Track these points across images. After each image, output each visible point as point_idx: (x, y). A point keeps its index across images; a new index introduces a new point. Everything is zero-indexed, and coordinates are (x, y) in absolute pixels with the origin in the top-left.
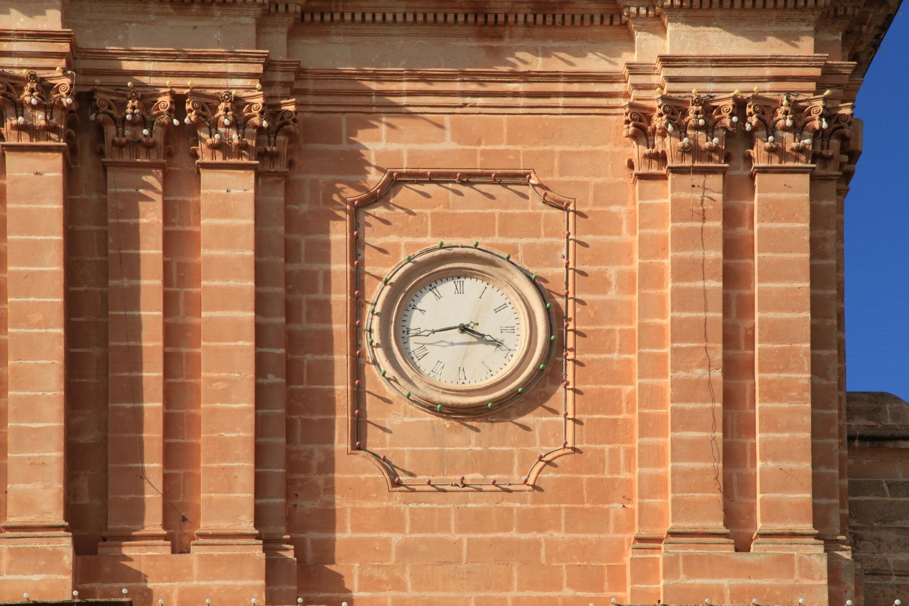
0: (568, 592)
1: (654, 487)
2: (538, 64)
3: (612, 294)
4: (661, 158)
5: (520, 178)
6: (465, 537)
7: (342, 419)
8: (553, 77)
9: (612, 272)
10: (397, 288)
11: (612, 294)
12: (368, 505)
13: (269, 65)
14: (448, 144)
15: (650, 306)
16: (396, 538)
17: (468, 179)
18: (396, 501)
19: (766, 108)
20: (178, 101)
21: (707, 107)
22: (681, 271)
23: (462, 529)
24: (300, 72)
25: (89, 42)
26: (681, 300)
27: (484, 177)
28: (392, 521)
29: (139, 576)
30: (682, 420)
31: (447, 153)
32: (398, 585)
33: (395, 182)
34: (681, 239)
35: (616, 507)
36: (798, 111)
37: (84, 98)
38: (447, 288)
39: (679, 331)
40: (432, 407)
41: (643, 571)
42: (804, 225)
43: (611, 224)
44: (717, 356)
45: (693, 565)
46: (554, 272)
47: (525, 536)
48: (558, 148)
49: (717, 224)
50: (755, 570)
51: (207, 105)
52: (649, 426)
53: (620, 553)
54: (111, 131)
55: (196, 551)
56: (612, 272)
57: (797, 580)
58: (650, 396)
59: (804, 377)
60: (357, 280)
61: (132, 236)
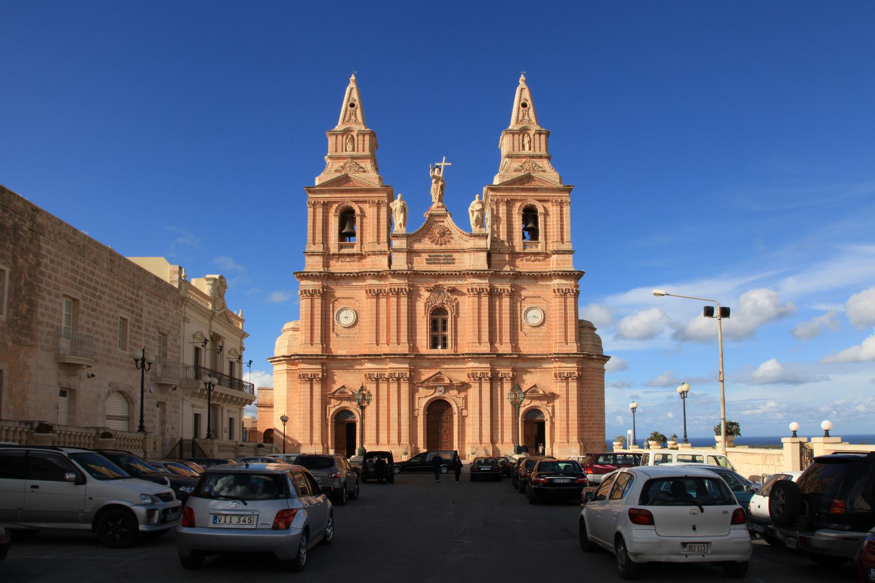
1: (556, 336)
2: (542, 283)
3: (551, 312)
4: (557, 295)
5: (540, 297)
7: (519, 328)
8: (544, 285)
9: (551, 309)
10: (526, 311)
11: (551, 312)
13: (511, 285)
14: (531, 293)
15: (556, 314)
17: (534, 297)
18: (526, 338)
19: (569, 290)
20: (501, 289)
21: (562, 290)
22: (560, 309)
24: (514, 285)
25: (491, 283)
26: (559, 313)
27: (536, 297)
28: (525, 340)
29: (496, 348)
30: (560, 328)
31: (531, 294)
33: (525, 298)
34: (559, 306)
35: (552, 338)
36: (572, 290)
37: (491, 289)
38: (531, 311)
39: (560, 317)
40: (530, 326)
41: (555, 347)
42: (573, 304)
43: (551, 303)
44: (564, 320)
45: (561, 346)
46: (544, 309)
48: (544, 293)
49: (563, 304)
50: (568, 347)
51: (504, 290)
52: (556, 329)
53: (552, 344)
54: (493, 293)
56: (551, 309)
57: (574, 348)
58: (556, 325)
59: (574, 323)
60: (521, 310)
61: (495, 306)
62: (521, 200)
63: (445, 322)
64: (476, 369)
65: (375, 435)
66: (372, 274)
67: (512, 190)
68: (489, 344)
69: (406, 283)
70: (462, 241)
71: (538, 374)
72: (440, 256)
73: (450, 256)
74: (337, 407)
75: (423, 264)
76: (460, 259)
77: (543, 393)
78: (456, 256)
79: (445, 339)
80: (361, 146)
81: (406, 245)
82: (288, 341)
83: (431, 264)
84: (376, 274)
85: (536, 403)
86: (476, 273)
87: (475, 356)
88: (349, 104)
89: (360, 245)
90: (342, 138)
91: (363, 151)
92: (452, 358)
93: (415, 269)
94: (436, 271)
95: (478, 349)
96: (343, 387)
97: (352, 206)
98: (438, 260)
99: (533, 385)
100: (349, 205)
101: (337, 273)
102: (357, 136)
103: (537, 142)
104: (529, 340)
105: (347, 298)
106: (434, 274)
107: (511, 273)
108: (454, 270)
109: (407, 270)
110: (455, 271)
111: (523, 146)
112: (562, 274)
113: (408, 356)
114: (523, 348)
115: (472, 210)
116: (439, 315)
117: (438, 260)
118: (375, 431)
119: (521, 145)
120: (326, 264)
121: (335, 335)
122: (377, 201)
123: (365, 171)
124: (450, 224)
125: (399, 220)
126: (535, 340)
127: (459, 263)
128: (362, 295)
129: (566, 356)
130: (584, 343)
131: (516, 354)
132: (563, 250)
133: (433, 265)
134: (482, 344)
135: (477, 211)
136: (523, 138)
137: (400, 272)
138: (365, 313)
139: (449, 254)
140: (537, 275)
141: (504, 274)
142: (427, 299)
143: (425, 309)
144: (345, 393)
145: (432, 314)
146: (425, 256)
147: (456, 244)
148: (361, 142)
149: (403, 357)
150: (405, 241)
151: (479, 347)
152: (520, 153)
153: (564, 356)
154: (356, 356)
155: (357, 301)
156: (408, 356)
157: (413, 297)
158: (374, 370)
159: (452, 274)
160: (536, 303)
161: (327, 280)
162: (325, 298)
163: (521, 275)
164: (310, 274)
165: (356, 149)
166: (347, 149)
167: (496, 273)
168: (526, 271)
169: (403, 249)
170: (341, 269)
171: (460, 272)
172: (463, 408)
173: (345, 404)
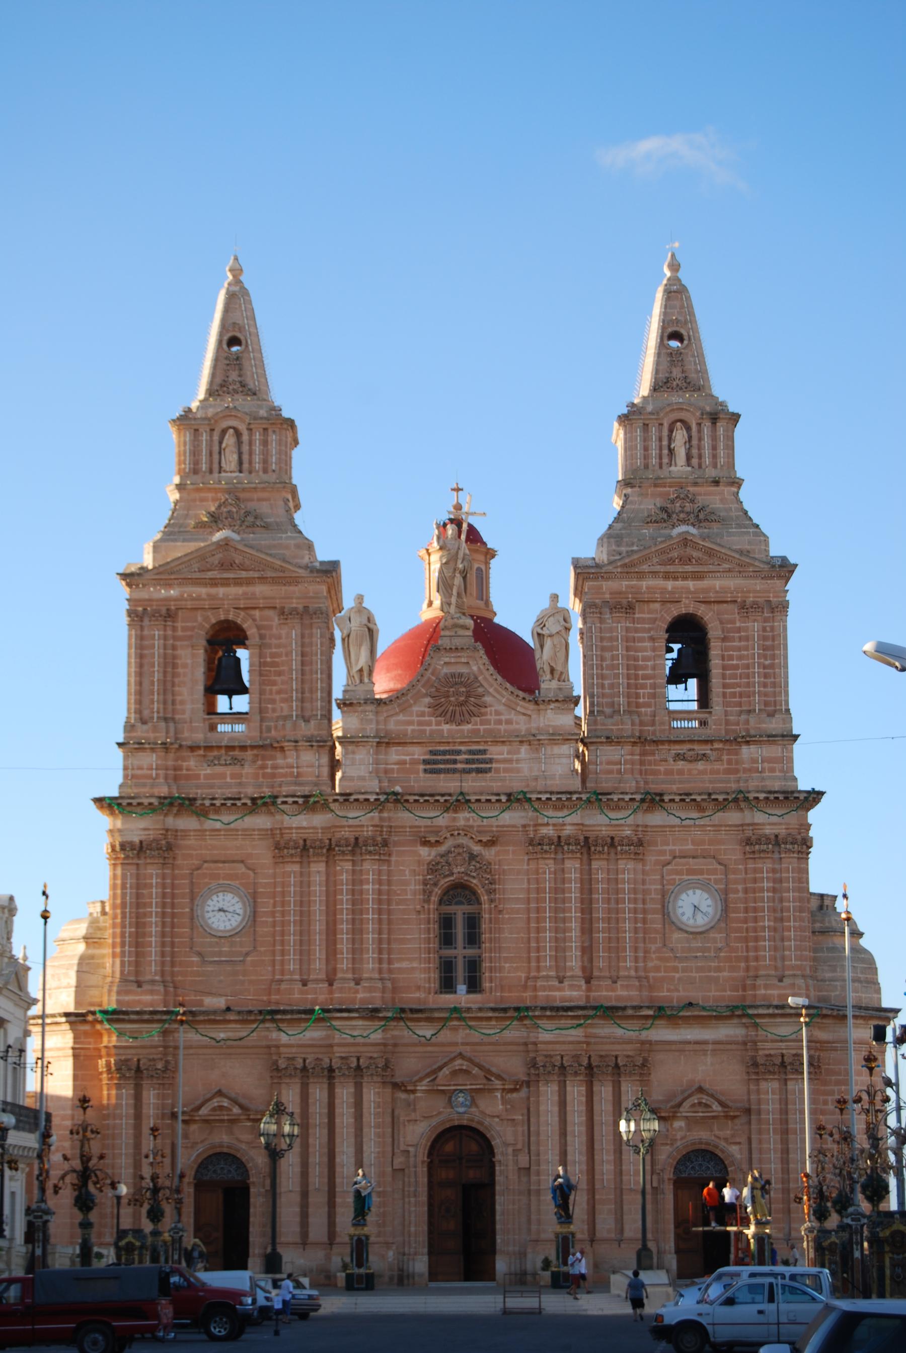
0: (729, 993)
6: (697, 975)
12: (668, 964)
16: (677, 975)
23: (697, 972)
28: (675, 969)
32: (679, 991)
47: (715, 974)
55: (619, 983)
62: (664, 602)
63: (473, 923)
64: (550, 1047)
65: (298, 1219)
66: (290, 800)
67: (641, 575)
68: (583, 982)
69: (377, 826)
70: (513, 716)
71: (709, 1059)
72: (459, 752)
73: (484, 752)
74: (200, 1148)
75: (418, 773)
76: (510, 761)
77: (720, 1109)
78: (496, 752)
79: (473, 966)
80: (257, 458)
81: (373, 726)
82: (78, 971)
83: (438, 772)
84: (301, 801)
85: (702, 1135)
86: (549, 799)
87: (548, 1013)
88: (226, 338)
89: (258, 724)
90: (211, 436)
91: (265, 471)
92: (489, 1019)
93: (398, 789)
94: (450, 795)
95: (557, 994)
96: (220, 1093)
97: (239, 621)
98: (455, 762)
99: (697, 1086)
100: (231, 617)
101: (204, 799)
102: (250, 430)
103: (707, 442)
104: (685, 970)
105: (224, 862)
106: (446, 801)
107: (638, 797)
108: (495, 791)
109: (377, 794)
110: (498, 795)
111: (671, 451)
112: (767, 798)
113: (381, 1015)
114: (669, 990)
115: (540, 631)
116: (459, 903)
117: (455, 762)
118: (297, 1209)
119: (665, 452)
120: (176, 776)
121: (195, 959)
122: (300, 607)
123: (266, 527)
124: (484, 671)
125: (357, 661)
126: (700, 969)
127: (506, 770)
128: (262, 853)
129: (776, 1011)
130: (828, 975)
131: (649, 1008)
132: (769, 732)
133: (442, 776)
134: (566, 983)
135: (551, 636)
136: (671, 431)
137: (361, 797)
138: (272, 901)
139: (481, 748)
140: (703, 800)
141: (619, 799)
142: (429, 864)
143: (424, 891)
144: (221, 1108)
145: (440, 902)
146: (418, 753)
147: (499, 722)
148: (257, 448)
149: (372, 1014)
150: (371, 716)
151: (559, 990)
152: (663, 473)
153: (771, 1011)
154: (250, 1012)
155: (253, 870)
156: (381, 1015)
157: (393, 859)
158: (294, 1050)
159: (489, 801)
160: (701, 872)
161: (176, 815)
162: (171, 861)
163: (663, 801)
164: (134, 802)
165: (246, 466)
166: (223, 464)
167: (600, 797)
168: (674, 787)
169: (367, 737)
170: (212, 786)
171: (509, 795)
172: (519, 1146)
173: (223, 1138)
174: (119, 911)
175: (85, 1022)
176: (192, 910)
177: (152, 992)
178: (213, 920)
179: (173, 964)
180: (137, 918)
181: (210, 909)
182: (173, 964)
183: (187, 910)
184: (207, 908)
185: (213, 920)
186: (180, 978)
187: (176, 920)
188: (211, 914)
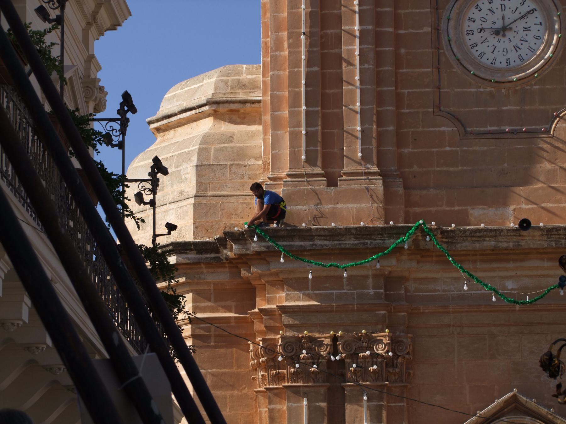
174: (285, 34)
175: (218, 263)
176: (437, 29)
177: (355, 196)
178: (481, 48)
179: (400, 142)
180: (323, 46)
181: (474, 27)
182: (400, 142)
183: (427, 29)
184: (467, 25)
185: (481, 48)
186: (415, 168)
187: (403, 51)
188: (476, 37)
